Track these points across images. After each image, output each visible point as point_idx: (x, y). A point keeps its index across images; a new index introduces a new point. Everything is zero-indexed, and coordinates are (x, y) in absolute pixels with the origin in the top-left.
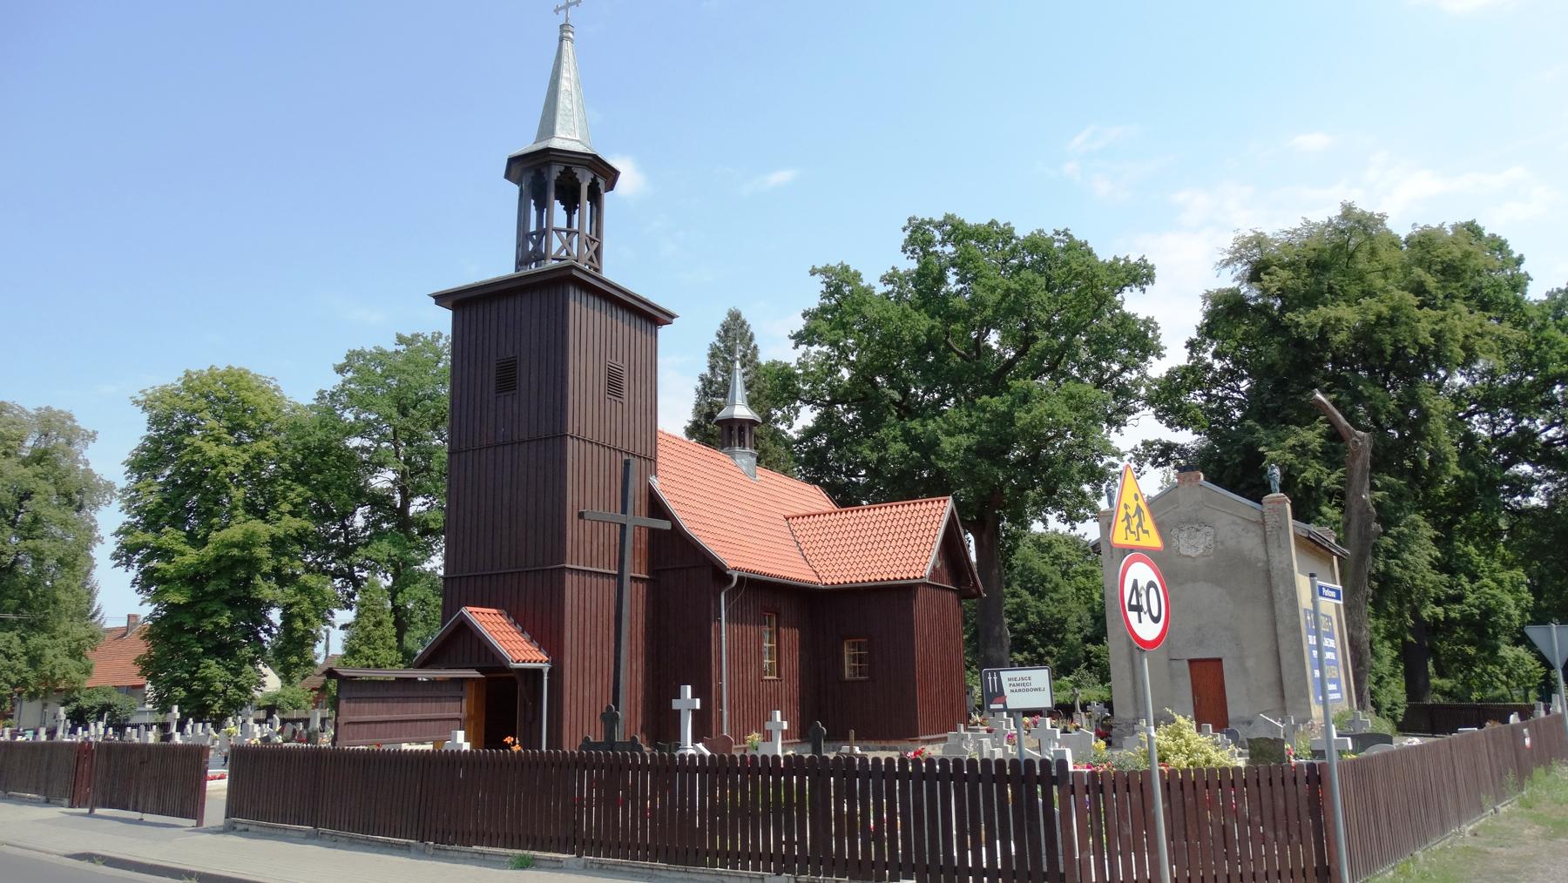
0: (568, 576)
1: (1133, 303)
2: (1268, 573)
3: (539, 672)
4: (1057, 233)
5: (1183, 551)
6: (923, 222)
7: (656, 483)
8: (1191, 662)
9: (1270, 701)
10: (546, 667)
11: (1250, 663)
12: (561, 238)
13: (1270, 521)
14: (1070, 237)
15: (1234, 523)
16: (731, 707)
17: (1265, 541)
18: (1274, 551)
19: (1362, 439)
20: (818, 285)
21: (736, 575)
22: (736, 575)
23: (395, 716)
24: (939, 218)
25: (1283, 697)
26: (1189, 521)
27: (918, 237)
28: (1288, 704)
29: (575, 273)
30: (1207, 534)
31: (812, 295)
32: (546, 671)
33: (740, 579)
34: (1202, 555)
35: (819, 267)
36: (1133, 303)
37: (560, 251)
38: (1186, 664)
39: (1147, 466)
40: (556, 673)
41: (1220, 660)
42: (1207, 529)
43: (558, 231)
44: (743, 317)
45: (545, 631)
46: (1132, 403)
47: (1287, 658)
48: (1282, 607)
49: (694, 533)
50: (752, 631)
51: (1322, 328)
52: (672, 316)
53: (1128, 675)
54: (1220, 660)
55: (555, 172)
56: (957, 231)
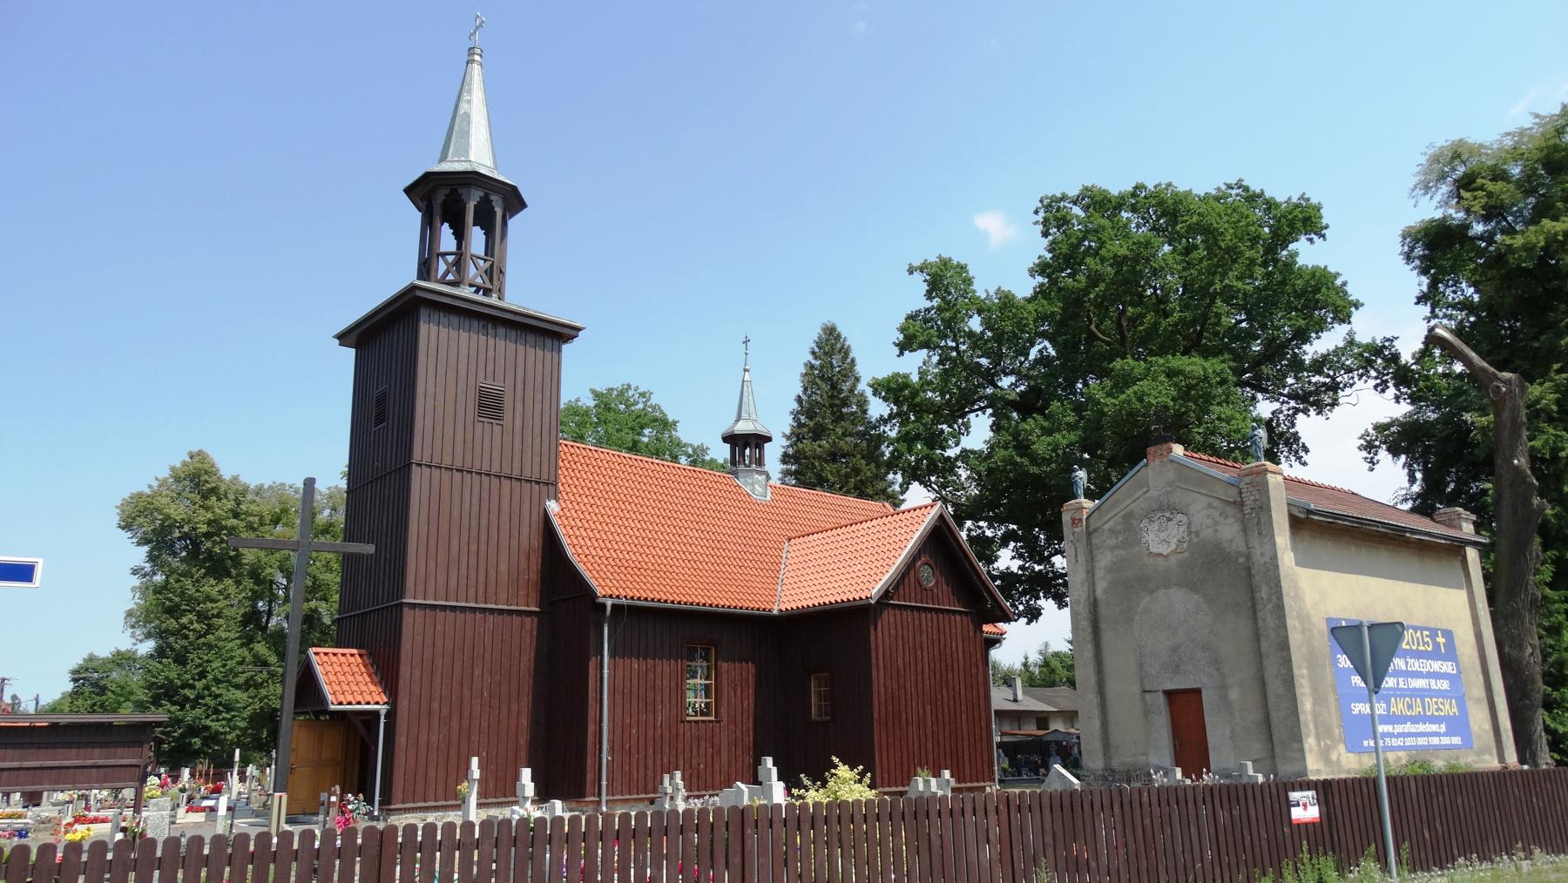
0: (408, 615)
1: (1307, 253)
2: (1249, 569)
3: (376, 714)
4: (1230, 187)
6: (1054, 200)
7: (553, 507)
8: (1170, 694)
9: (1258, 748)
10: (383, 709)
11: (1234, 695)
12: (446, 262)
13: (1249, 501)
14: (1246, 189)
15: (1210, 506)
16: (612, 750)
17: (1245, 530)
18: (1255, 542)
19: (1507, 382)
20: (919, 284)
21: (609, 602)
22: (609, 602)
23: (90, 762)
24: (1073, 192)
25: (1271, 741)
26: (1161, 509)
27: (1053, 214)
28: (1277, 750)
29: (419, 293)
30: (1179, 523)
31: (915, 297)
32: (383, 713)
33: (613, 606)
34: (1175, 552)
35: (916, 263)
36: (1307, 253)
37: (447, 273)
38: (1161, 699)
39: (1383, 455)
40: (389, 715)
41: (1198, 691)
42: (1180, 517)
43: (444, 255)
44: (839, 329)
45: (386, 671)
46: (1342, 378)
47: (1274, 686)
48: (1266, 615)
49: (574, 559)
50: (665, 667)
51: (1545, 249)
52: (579, 329)
53: (1096, 712)
54: (1198, 691)
55: (440, 197)
56: (1097, 202)
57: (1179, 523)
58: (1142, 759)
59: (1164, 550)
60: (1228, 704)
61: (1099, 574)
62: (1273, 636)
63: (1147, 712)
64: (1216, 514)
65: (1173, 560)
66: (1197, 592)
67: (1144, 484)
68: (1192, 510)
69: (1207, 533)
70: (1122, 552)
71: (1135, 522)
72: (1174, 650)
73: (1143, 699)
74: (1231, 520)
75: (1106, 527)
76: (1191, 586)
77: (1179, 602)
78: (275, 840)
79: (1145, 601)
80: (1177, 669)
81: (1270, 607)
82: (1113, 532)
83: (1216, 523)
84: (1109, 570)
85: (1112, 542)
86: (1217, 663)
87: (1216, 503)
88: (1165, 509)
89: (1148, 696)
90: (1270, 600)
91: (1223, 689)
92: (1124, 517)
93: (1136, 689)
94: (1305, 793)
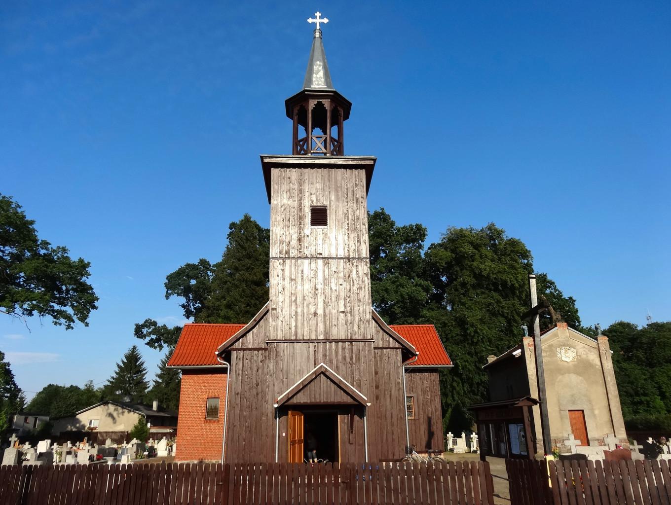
5: (564, 359)
11: (596, 412)
15: (584, 347)
26: (564, 345)
42: (573, 349)
58: (560, 435)
60: (595, 416)
62: (613, 393)
63: (562, 418)
64: (587, 351)
65: (571, 364)
66: (581, 376)
67: (556, 335)
68: (577, 347)
69: (584, 356)
70: (549, 359)
71: (554, 349)
72: (572, 396)
73: (560, 413)
74: (592, 353)
76: (579, 374)
77: (574, 379)
78: (463, 466)
79: (560, 377)
80: (574, 403)
81: (611, 383)
83: (587, 353)
86: (590, 401)
87: (587, 346)
88: (567, 345)
89: (562, 412)
90: (611, 381)
91: (592, 410)
93: (557, 409)
94: (423, 455)
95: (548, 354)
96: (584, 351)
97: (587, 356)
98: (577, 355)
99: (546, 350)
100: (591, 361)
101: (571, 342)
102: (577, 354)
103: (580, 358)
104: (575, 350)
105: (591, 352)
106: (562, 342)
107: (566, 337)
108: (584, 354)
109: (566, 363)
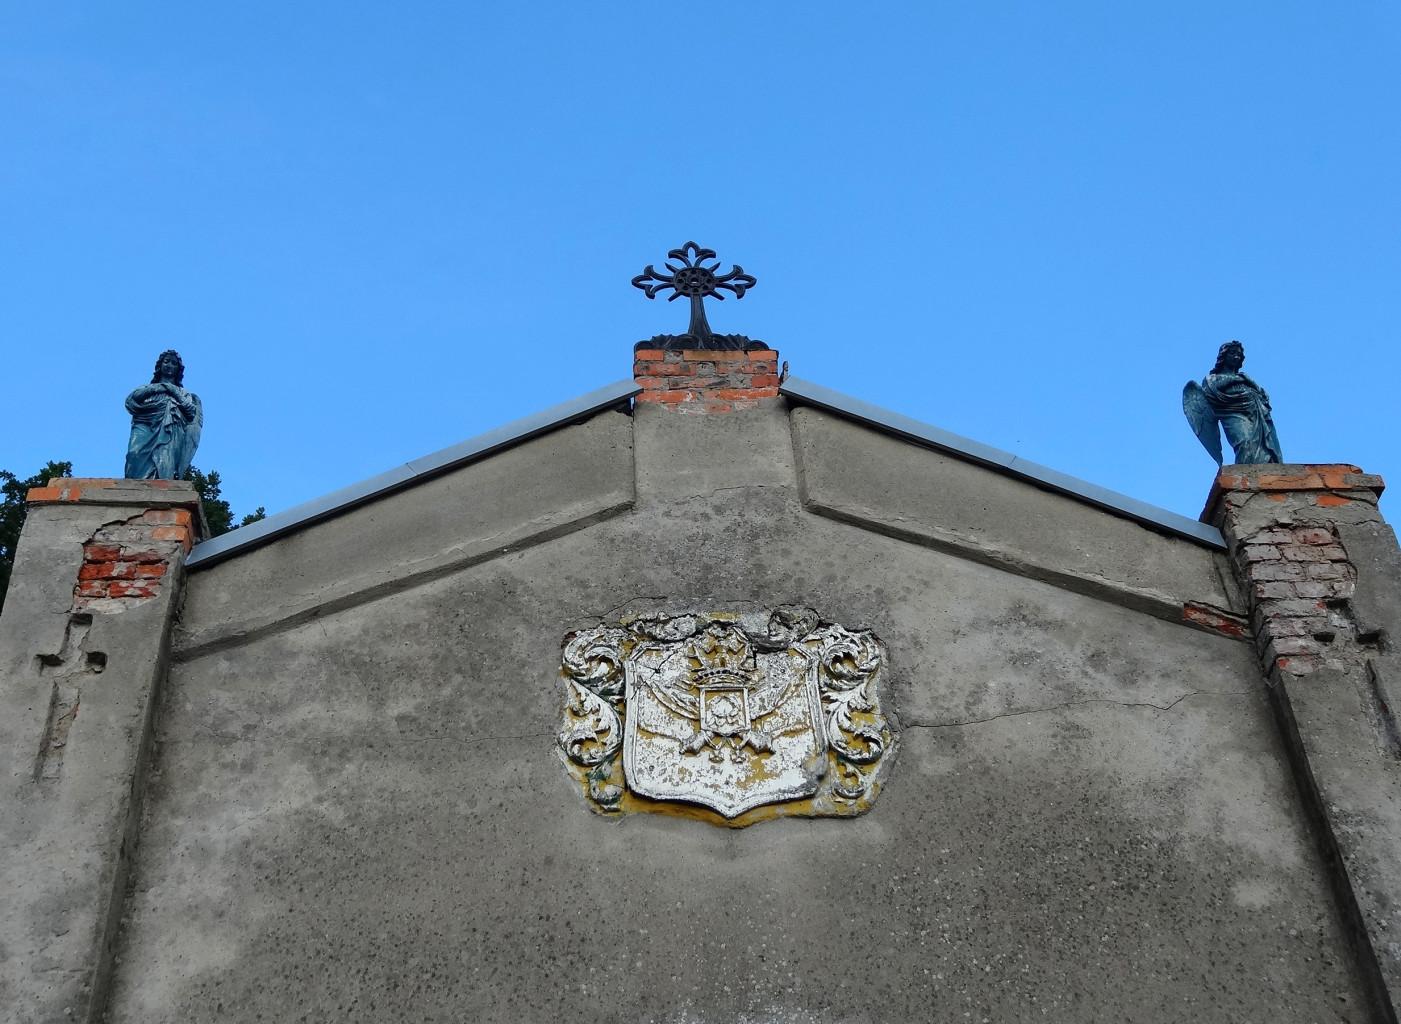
5: (657, 768)
15: (1020, 615)
26: (702, 589)
30: (835, 673)
57: (835, 673)
59: (721, 785)
61: (180, 883)
64: (1070, 659)
65: (778, 849)
68: (906, 619)
69: (1019, 739)
70: (401, 778)
71: (523, 641)
74: (1150, 692)
75: (311, 636)
82: (354, 667)
83: (1072, 697)
84: (267, 867)
85: (353, 712)
87: (1061, 605)
92: (438, 604)
95: (394, 710)
96: (1019, 660)
97: (1074, 731)
98: (901, 725)
99: (397, 650)
100: (1138, 807)
101: (818, 553)
102: (894, 691)
103: (935, 765)
104: (869, 655)
105: (1130, 676)
106: (673, 559)
107: (749, 495)
108: (1011, 709)
109: (689, 837)
